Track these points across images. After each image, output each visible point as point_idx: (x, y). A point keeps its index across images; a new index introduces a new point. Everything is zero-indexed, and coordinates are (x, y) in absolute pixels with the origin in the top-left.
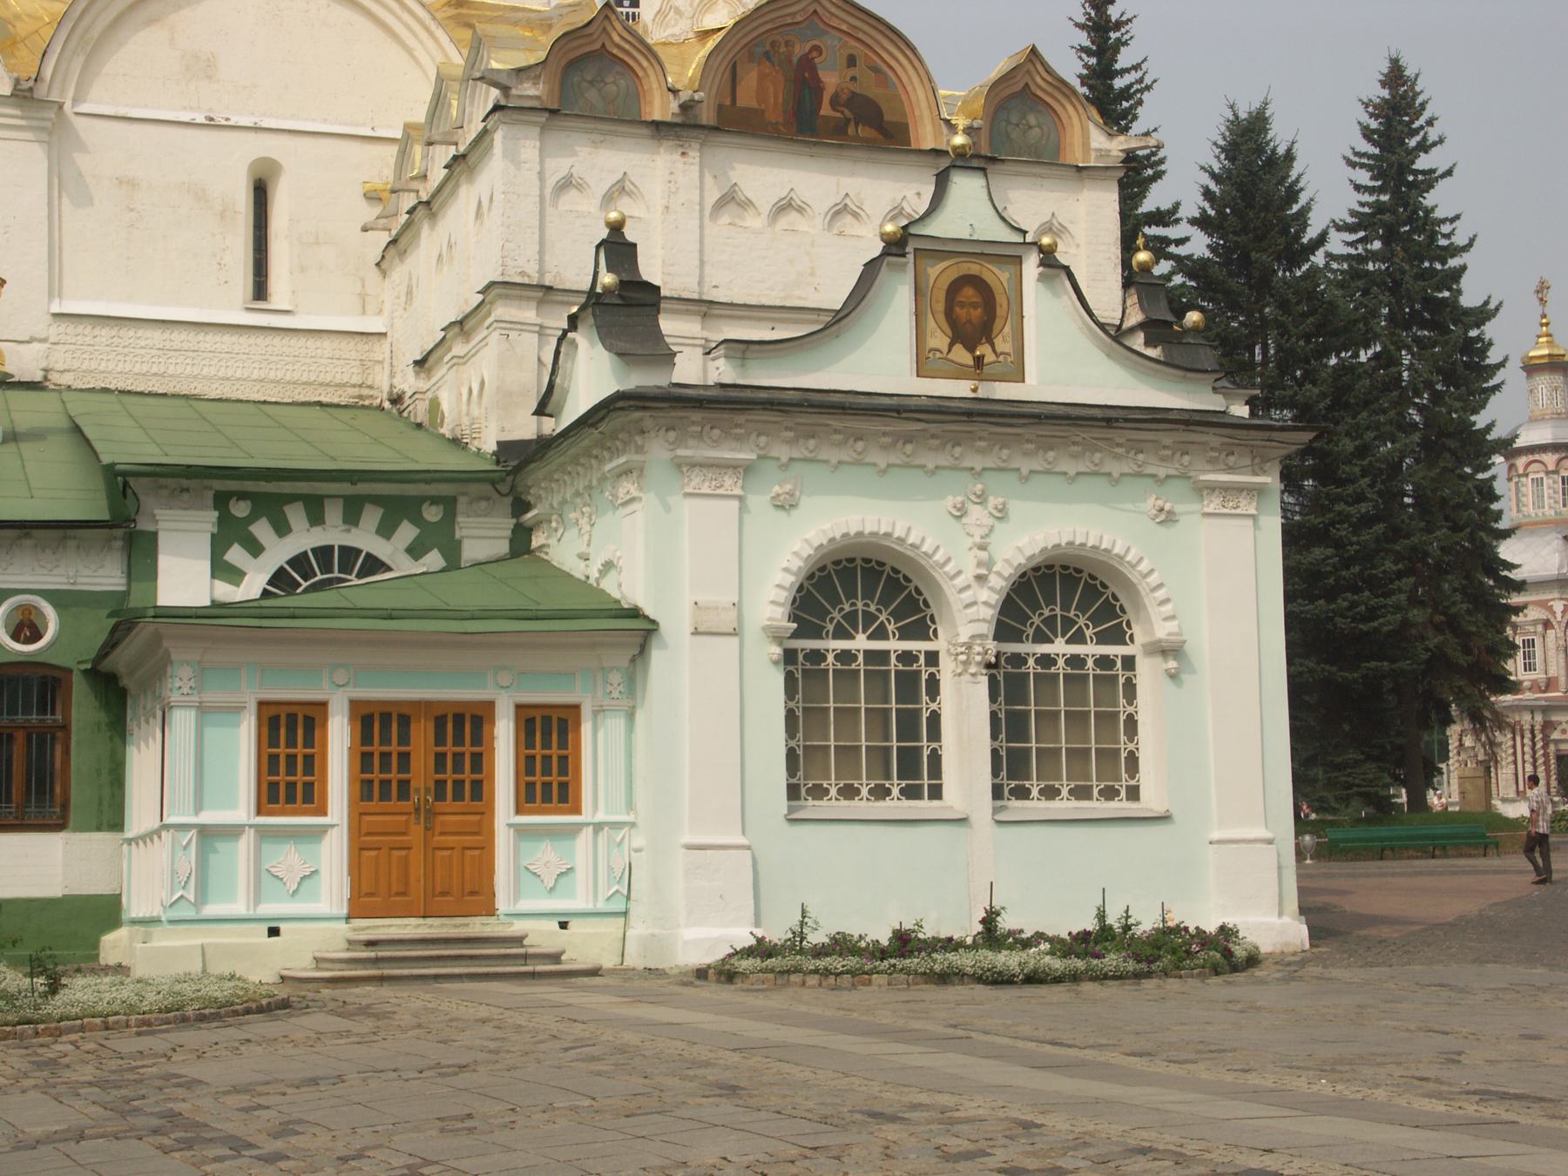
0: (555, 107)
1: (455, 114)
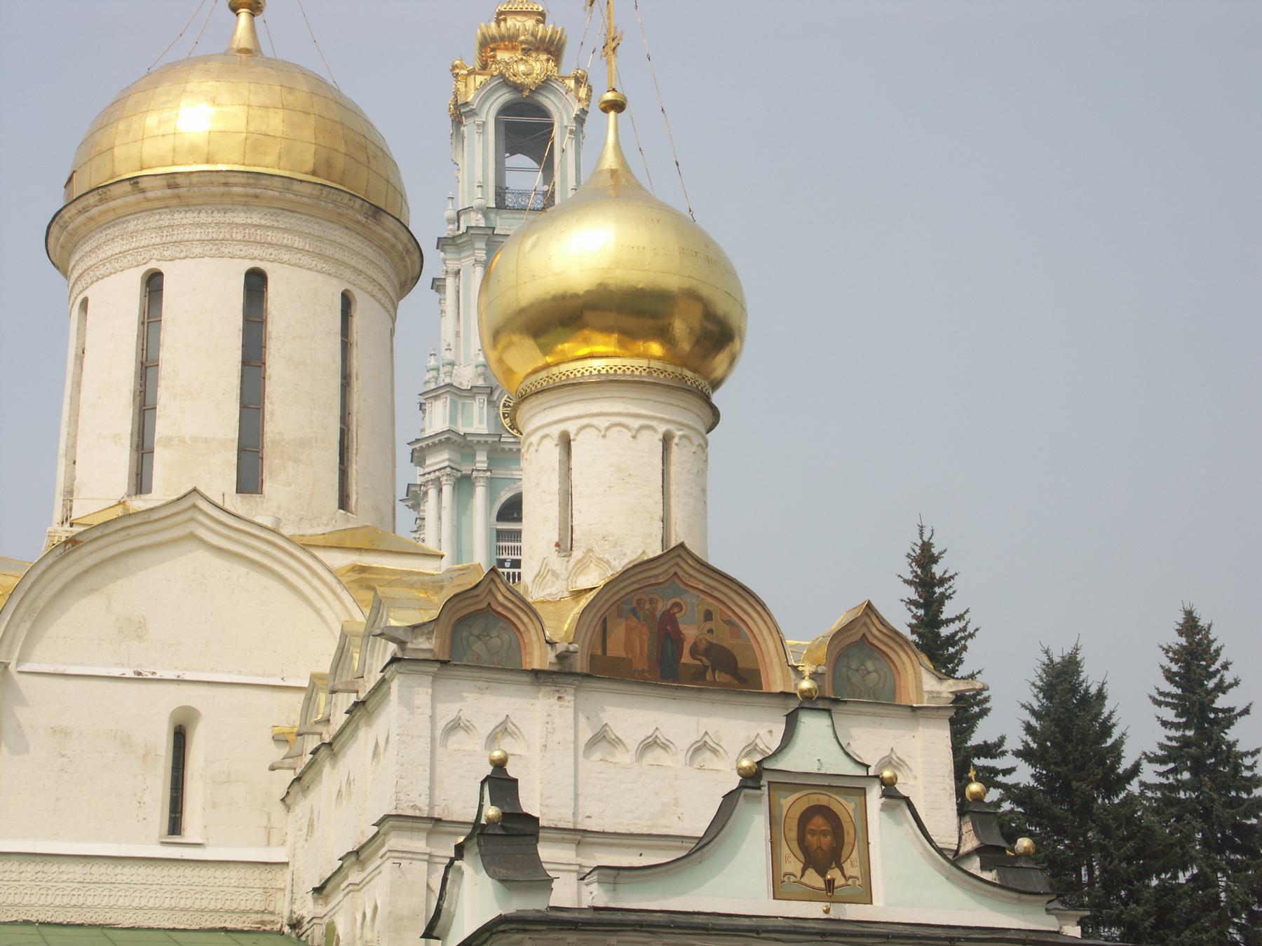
0: (446, 658)
1: (356, 665)
